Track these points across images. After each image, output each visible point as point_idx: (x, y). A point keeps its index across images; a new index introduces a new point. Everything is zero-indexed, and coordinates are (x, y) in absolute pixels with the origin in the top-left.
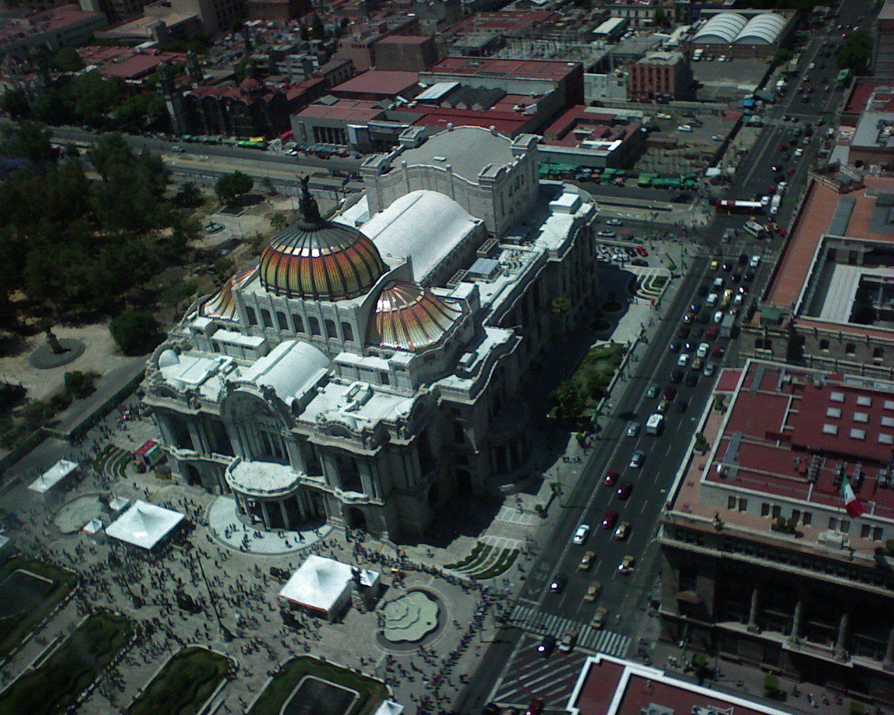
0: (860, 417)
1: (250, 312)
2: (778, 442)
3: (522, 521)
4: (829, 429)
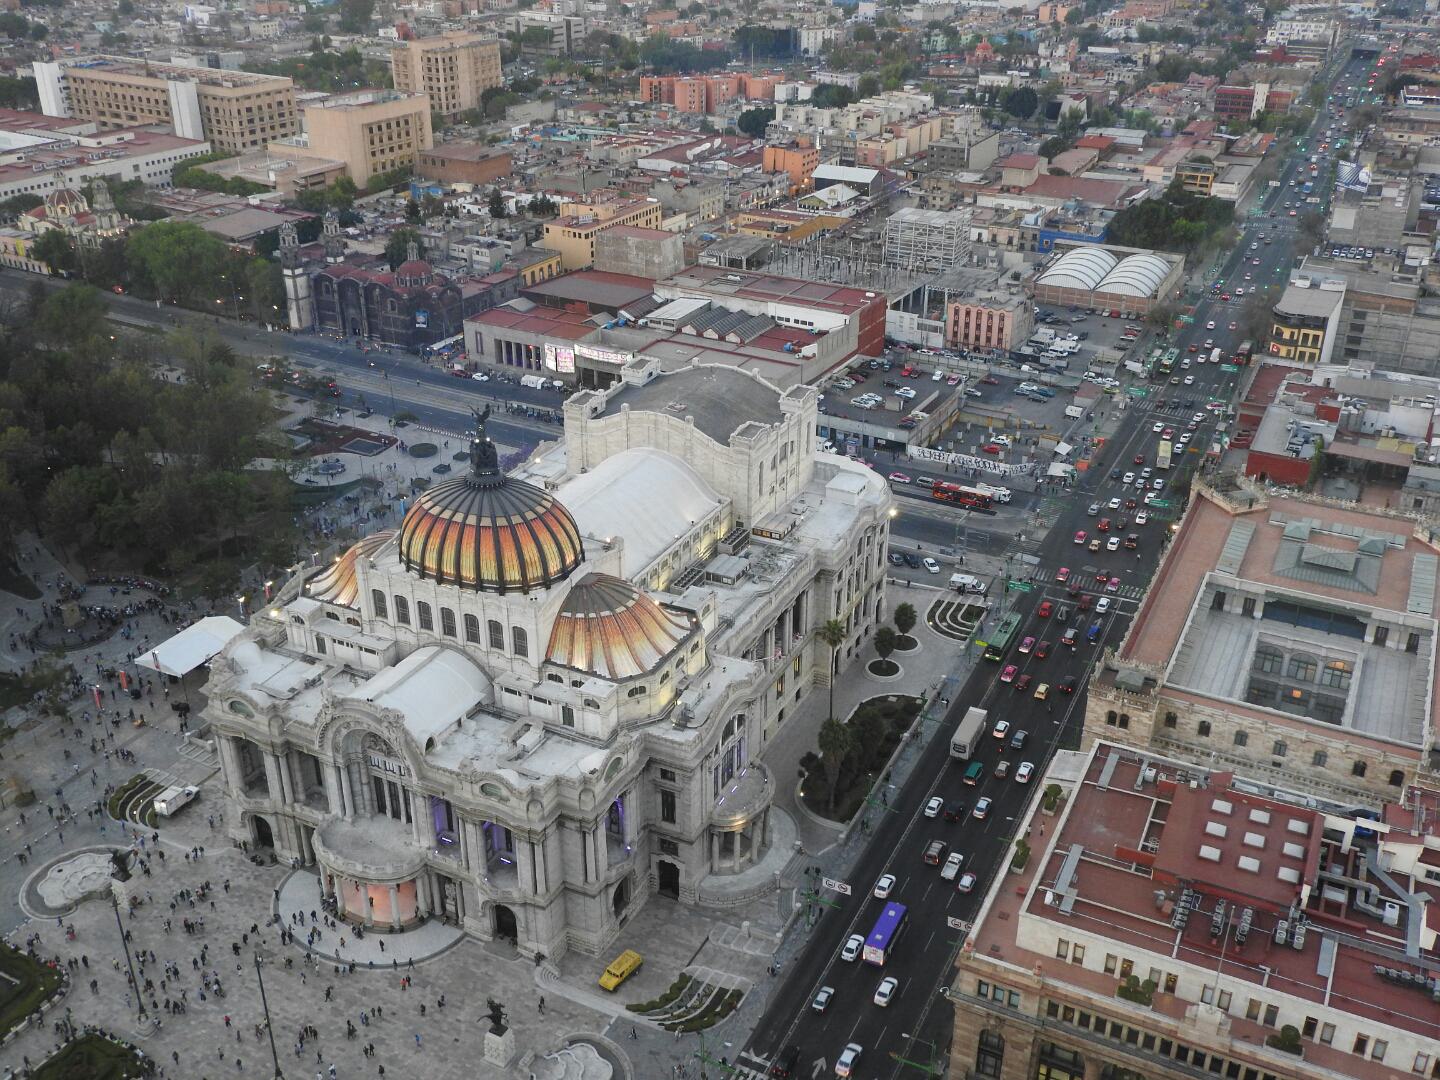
0: (1254, 839)
1: (379, 597)
2: (1134, 866)
3: (749, 948)
4: (1210, 852)
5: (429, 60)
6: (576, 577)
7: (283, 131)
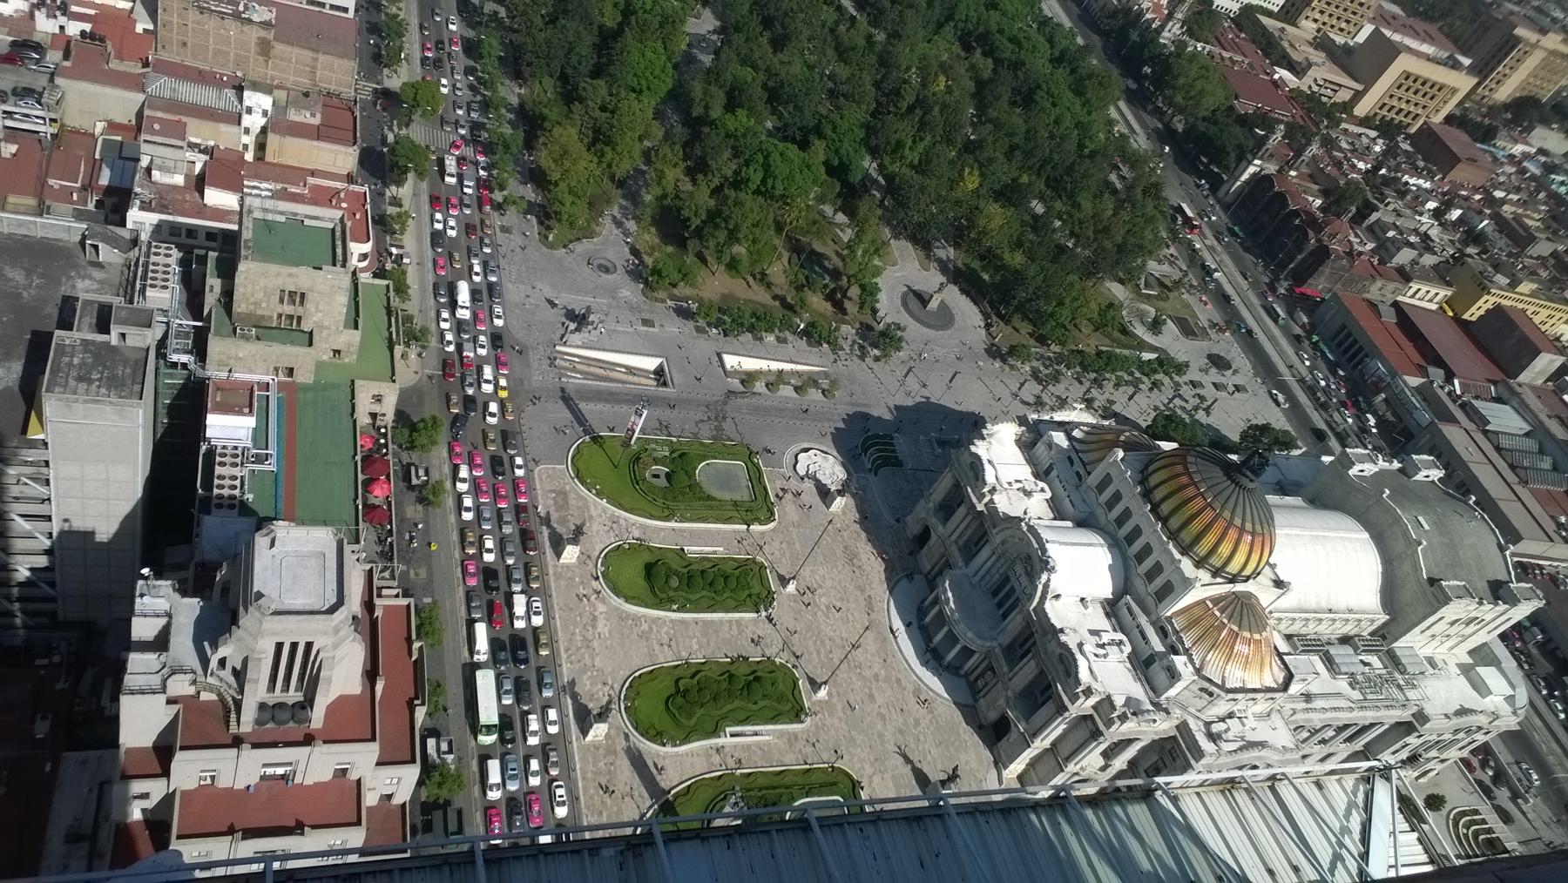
5: (1508, 41)
6: (1239, 587)
7: (1343, 25)
